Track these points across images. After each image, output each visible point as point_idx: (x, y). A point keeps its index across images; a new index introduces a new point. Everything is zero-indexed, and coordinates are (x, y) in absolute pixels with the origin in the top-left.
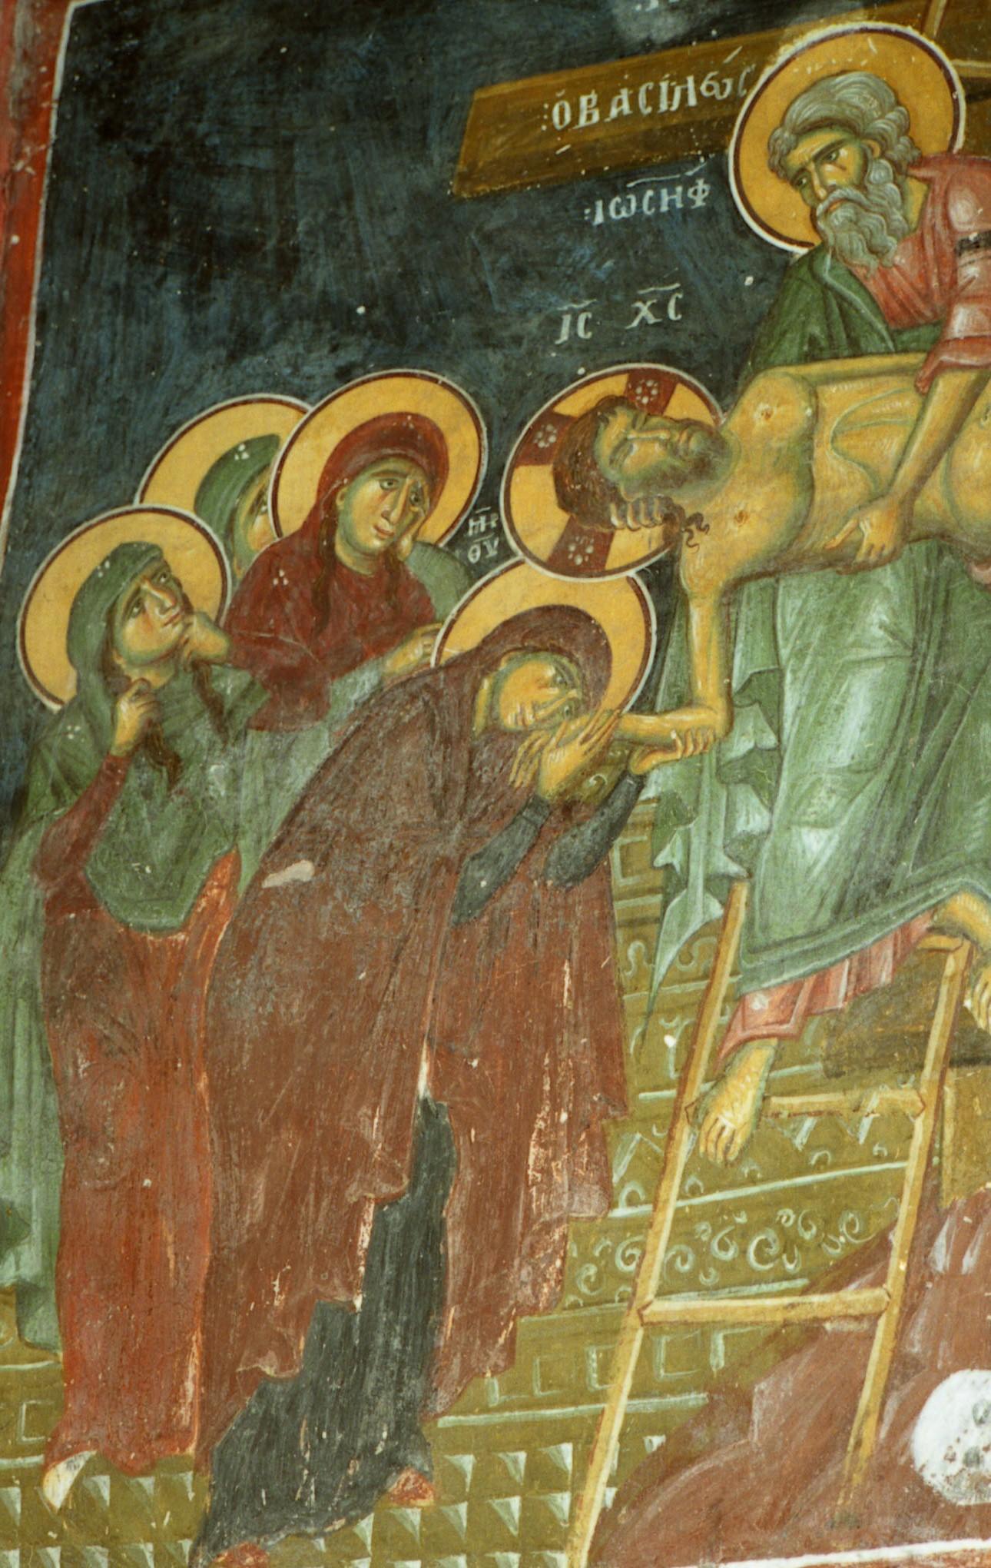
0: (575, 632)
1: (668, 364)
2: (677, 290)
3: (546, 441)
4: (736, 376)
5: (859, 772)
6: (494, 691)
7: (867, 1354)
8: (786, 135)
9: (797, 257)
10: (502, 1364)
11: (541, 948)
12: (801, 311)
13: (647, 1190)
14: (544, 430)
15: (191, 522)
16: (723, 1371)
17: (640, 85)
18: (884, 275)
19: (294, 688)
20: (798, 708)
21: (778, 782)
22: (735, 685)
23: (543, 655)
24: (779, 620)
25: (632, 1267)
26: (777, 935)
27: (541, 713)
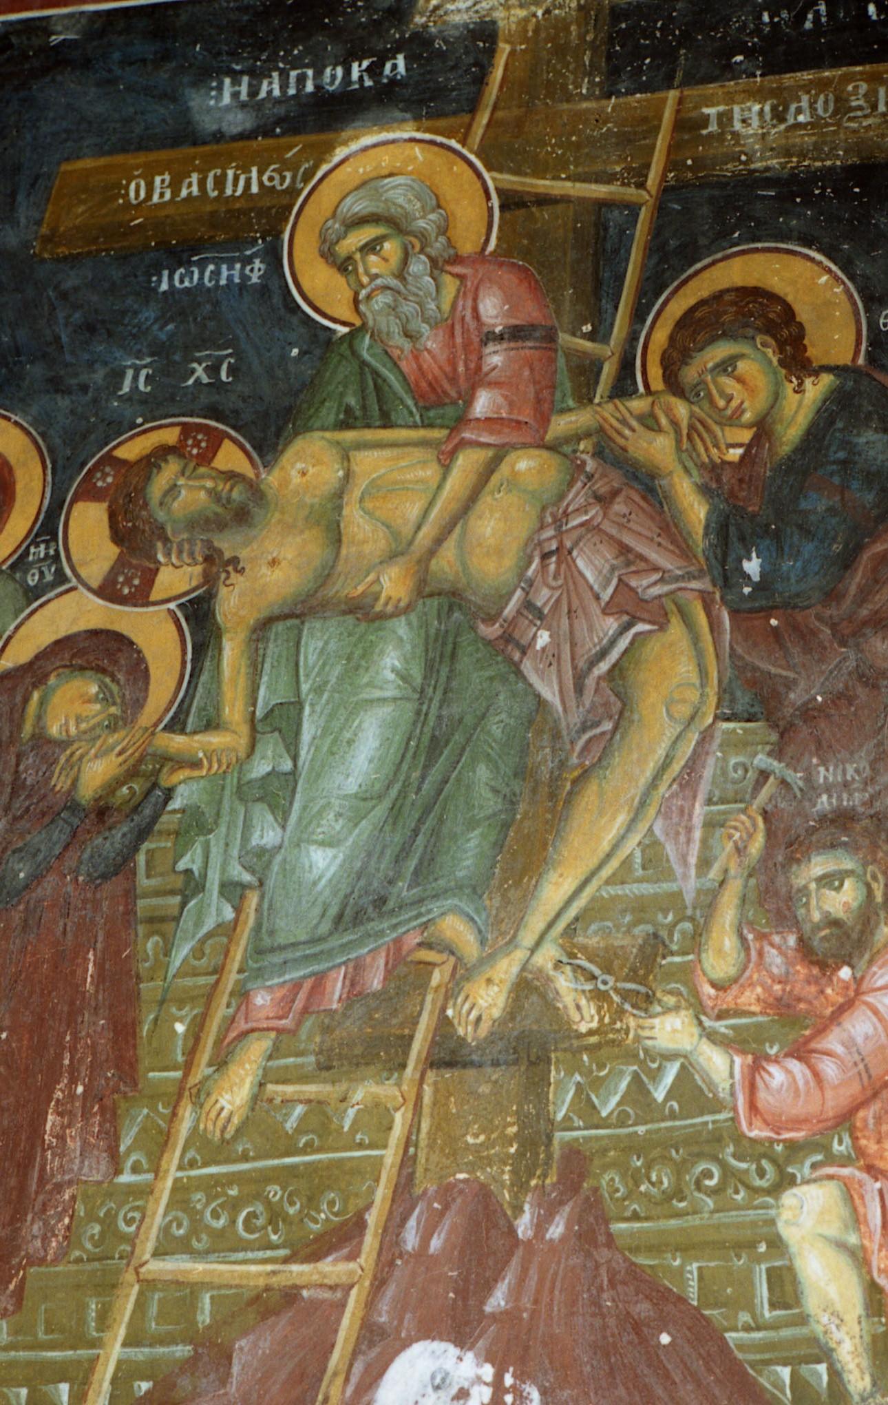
0: (119, 654)
1: (217, 420)
2: (230, 355)
3: (104, 481)
4: (278, 435)
5: (365, 799)
6: (42, 703)
7: (339, 1321)
8: (337, 226)
9: (340, 335)
10: (11, 1308)
11: (70, 936)
13: (150, 1161)
14: (102, 471)
16: (209, 1327)
17: (210, 170)
18: (416, 358)
20: (314, 738)
21: (291, 803)
22: (259, 713)
23: (89, 673)
24: (302, 658)
25: (133, 1228)
26: (281, 940)
27: (83, 726)
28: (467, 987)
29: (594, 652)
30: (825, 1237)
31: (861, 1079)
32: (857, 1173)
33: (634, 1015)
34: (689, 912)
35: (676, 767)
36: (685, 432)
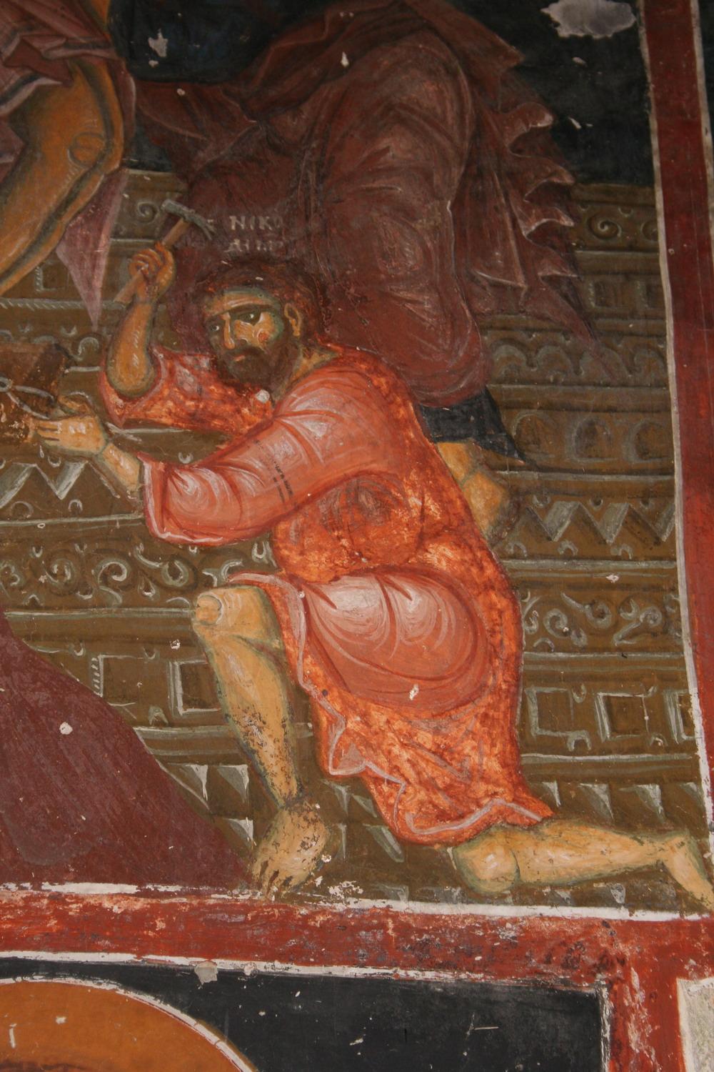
30: (245, 640)
31: (281, 493)
32: (278, 581)
33: (34, 417)
34: (95, 328)
35: (81, 203)
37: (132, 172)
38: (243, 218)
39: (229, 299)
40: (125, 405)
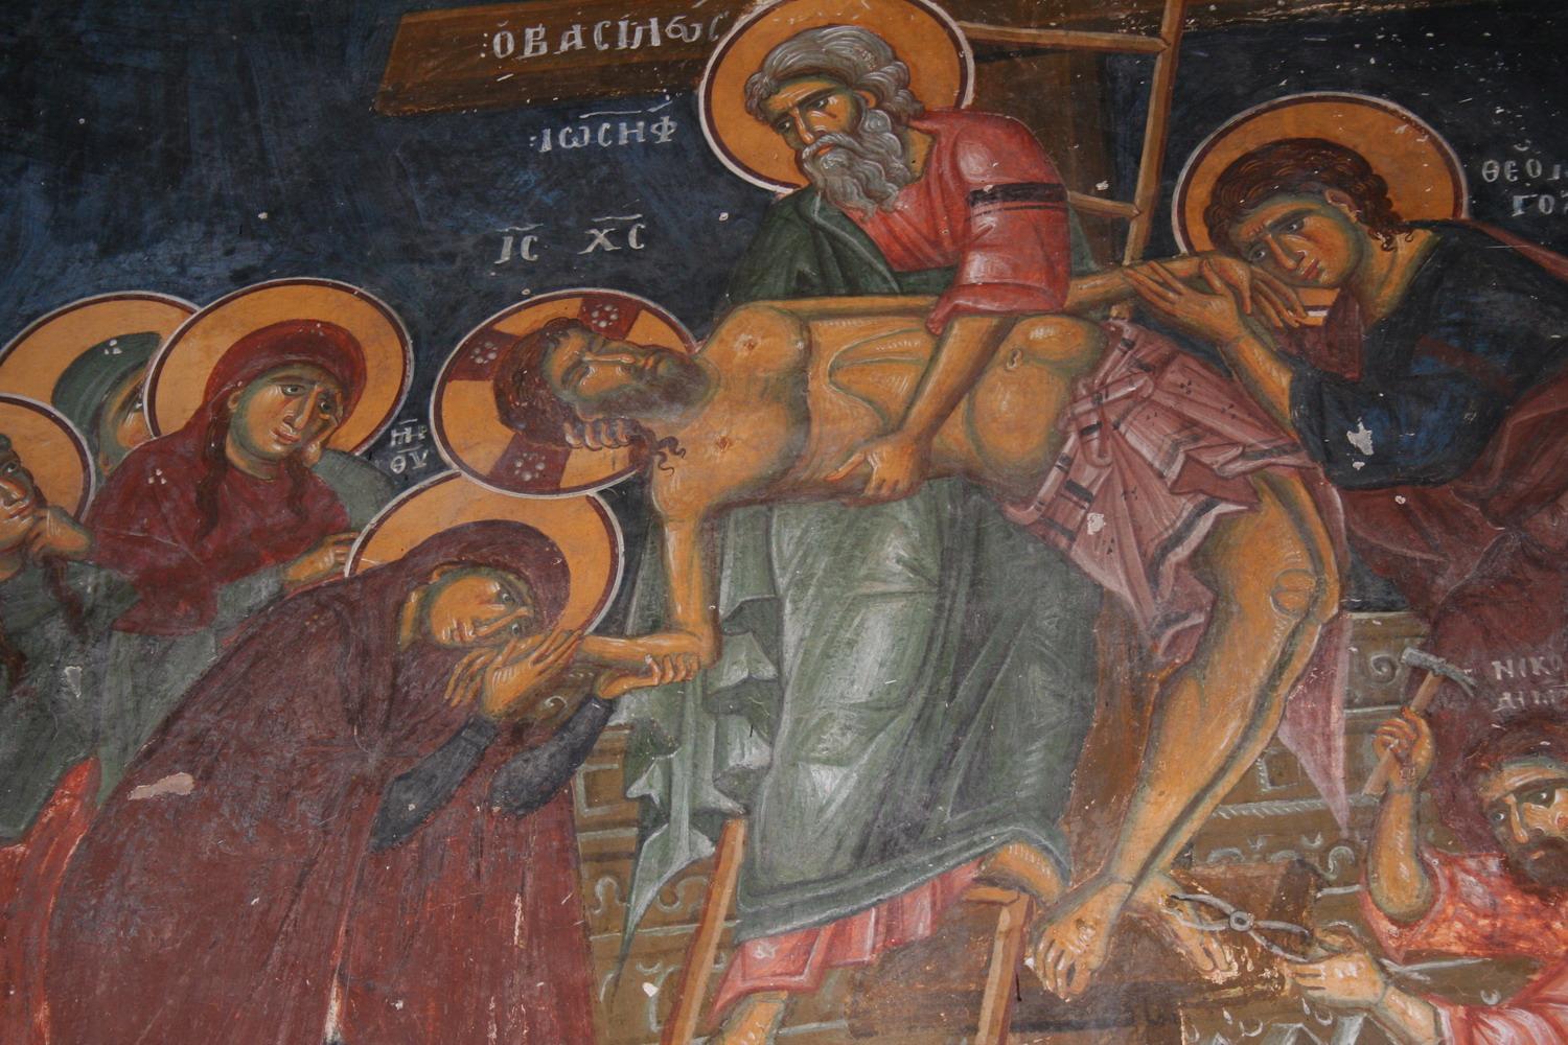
1: (630, 290)
5: (880, 709)
9: (781, 196)
11: (485, 879)
12: (786, 248)
15: (48, 414)
17: (596, 23)
19: (168, 595)
20: (802, 640)
21: (779, 716)
26: (784, 877)
27: (484, 630)
28: (1050, 931)
29: (1166, 536)
33: (1288, 961)
34: (1345, 834)
35: (1298, 665)
36: (1247, 294)
37: (1356, 616)
38: (1510, 663)
39: (1511, 775)
40: (1401, 934)
